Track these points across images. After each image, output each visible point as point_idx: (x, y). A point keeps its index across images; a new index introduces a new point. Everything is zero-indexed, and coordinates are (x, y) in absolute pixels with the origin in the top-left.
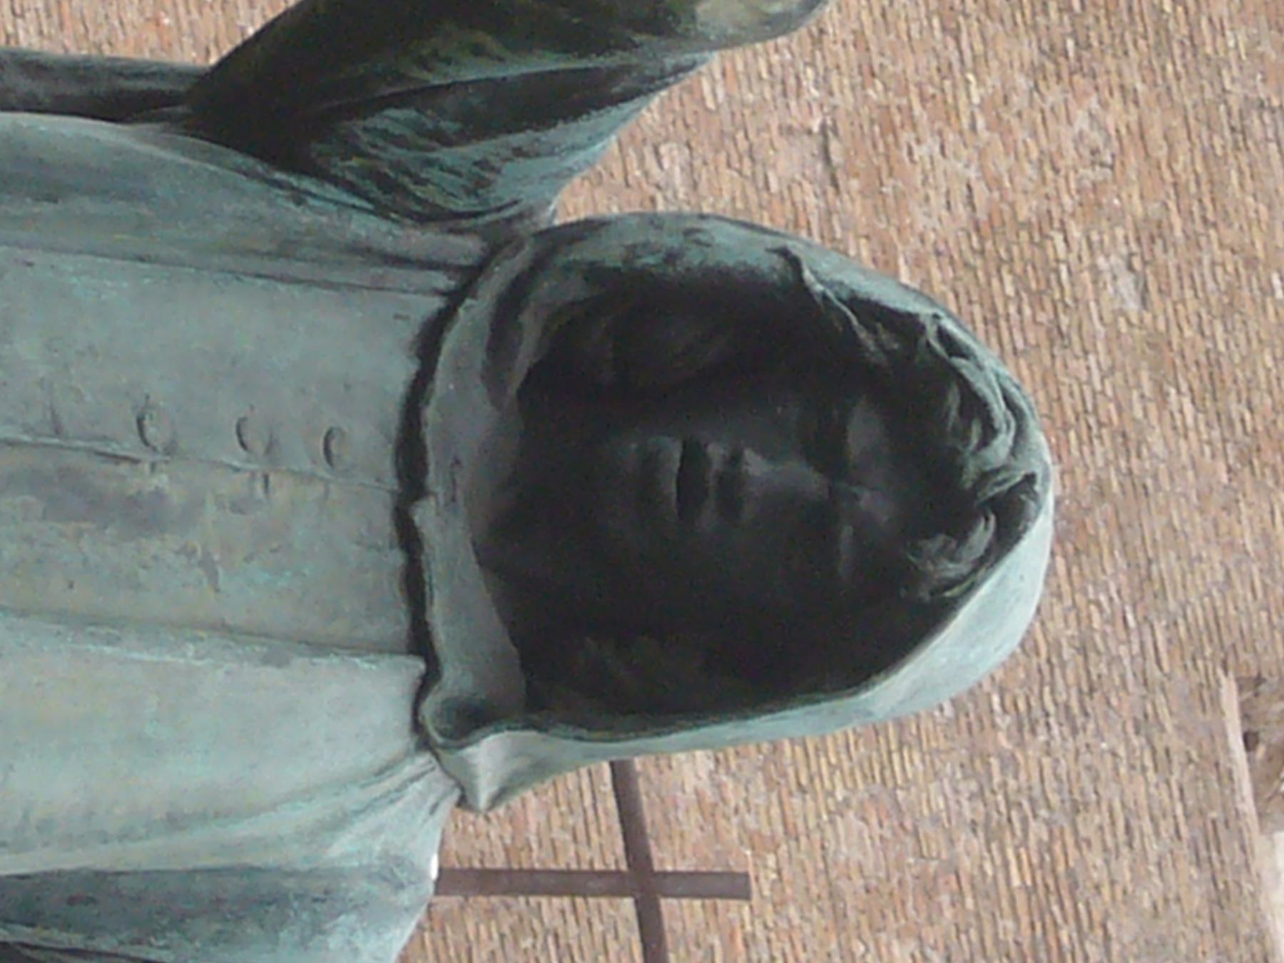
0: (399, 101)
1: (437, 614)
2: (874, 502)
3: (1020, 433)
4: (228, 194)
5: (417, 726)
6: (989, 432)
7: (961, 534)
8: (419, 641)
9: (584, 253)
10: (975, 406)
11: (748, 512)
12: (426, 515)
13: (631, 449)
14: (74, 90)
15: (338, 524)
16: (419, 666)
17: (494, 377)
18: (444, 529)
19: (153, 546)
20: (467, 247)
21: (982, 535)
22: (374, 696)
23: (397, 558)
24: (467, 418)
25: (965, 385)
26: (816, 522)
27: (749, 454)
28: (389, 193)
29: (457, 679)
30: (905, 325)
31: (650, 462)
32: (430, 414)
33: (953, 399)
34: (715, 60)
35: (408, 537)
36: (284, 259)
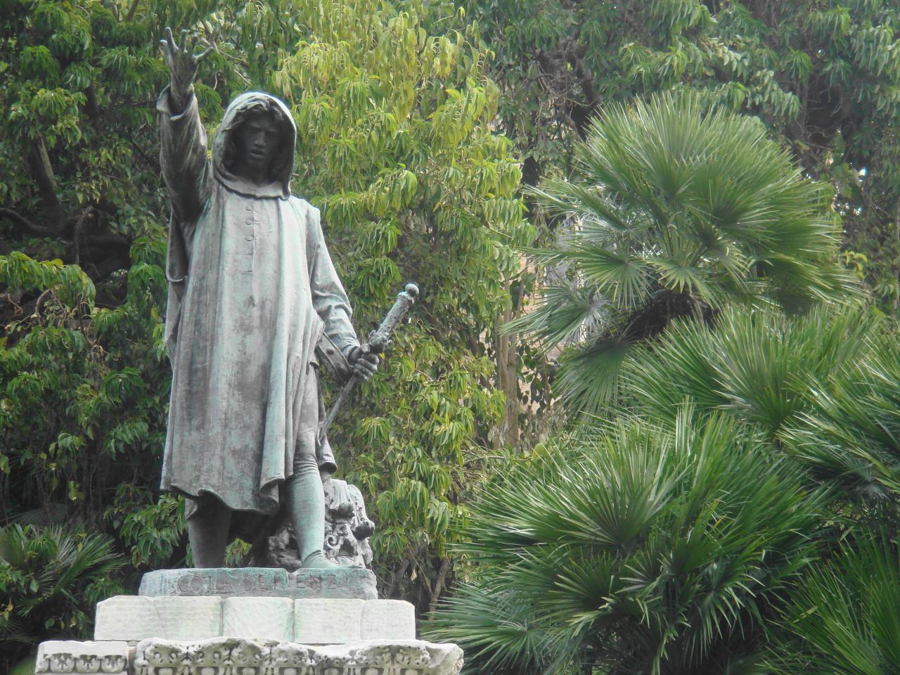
8: (276, 199)
9: (218, 164)
10: (256, 107)
20: (216, 182)
24: (240, 186)
27: (256, 142)
28: (209, 195)
29: (281, 193)
30: (238, 114)
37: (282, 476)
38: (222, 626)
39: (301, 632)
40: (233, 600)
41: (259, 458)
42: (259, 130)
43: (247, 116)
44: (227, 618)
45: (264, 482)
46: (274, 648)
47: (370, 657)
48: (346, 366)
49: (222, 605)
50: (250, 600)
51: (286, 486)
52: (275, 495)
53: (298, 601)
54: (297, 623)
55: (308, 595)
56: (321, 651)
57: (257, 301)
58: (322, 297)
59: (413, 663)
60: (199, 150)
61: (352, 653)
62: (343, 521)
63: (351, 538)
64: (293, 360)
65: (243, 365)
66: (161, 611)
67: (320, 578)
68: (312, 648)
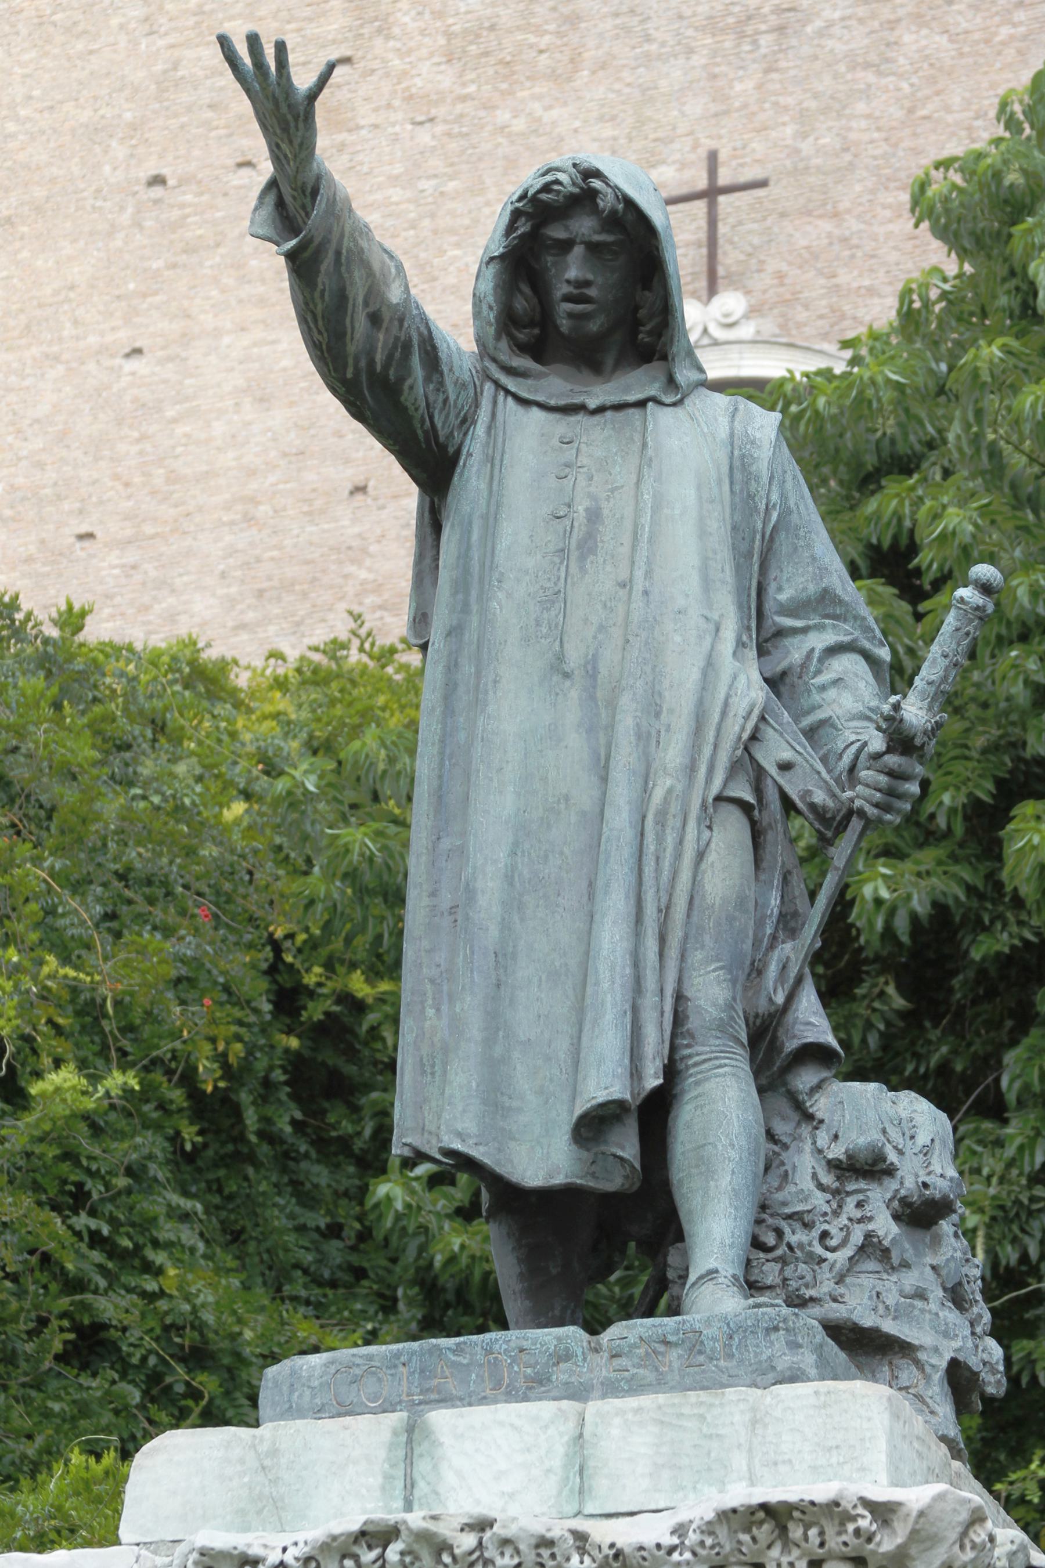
0: (431, 418)
1: (631, 398)
2: (584, 226)
3: (558, 169)
4: (471, 482)
5: (674, 405)
6: (557, 182)
7: (593, 193)
8: (641, 404)
9: (491, 343)
10: (546, 188)
11: (590, 277)
12: (592, 403)
13: (564, 325)
14: (430, 540)
15: (596, 438)
16: (650, 404)
17: (539, 376)
18: (597, 395)
19: (606, 512)
20: (488, 388)
21: (596, 184)
22: (666, 424)
23: (609, 414)
25: (539, 192)
26: (594, 248)
28: (467, 422)
30: (516, 214)
31: (571, 315)
32: (552, 402)
33: (544, 196)
34: (413, 291)
35: (601, 410)
36: (493, 460)
38: (410, 1485)
39: (601, 1484)
44: (422, 1466)
46: (488, 1535)
48: (833, 796)
49: (411, 1429)
50: (480, 1414)
51: (655, 1113)
52: (626, 1144)
53: (594, 1407)
54: (591, 1463)
55: (636, 1388)
58: (795, 631)
59: (834, 1542)
60: (386, 315)
61: (680, 1530)
62: (862, 1185)
63: (886, 1227)
64: (658, 795)
66: (267, 1462)
67: (666, 1343)
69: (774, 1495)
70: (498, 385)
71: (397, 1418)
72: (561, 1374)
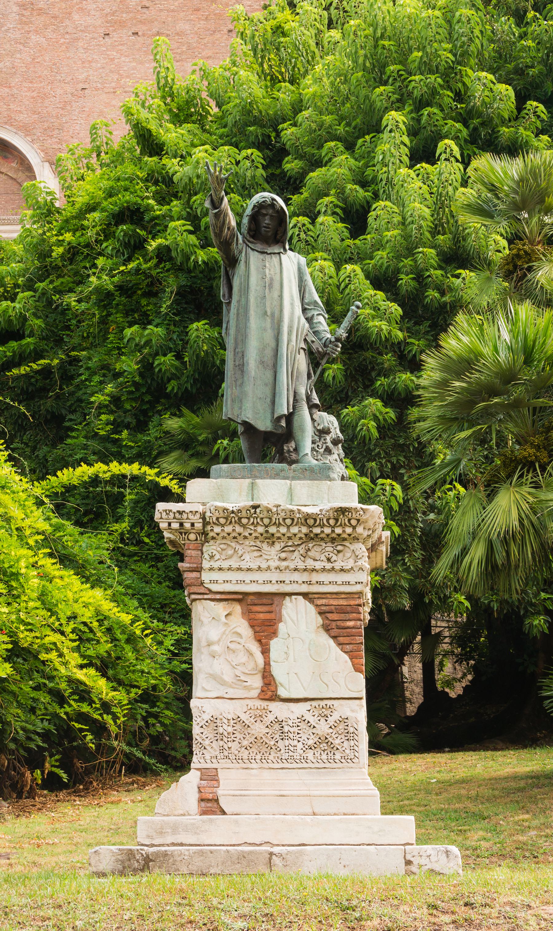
24: (259, 247)
28: (241, 252)
37: (286, 412)
38: (253, 495)
39: (295, 499)
40: (259, 481)
41: (273, 402)
42: (266, 215)
43: (260, 207)
44: (255, 492)
45: (276, 416)
47: (331, 512)
50: (268, 481)
53: (293, 482)
55: (299, 479)
56: (305, 510)
57: (269, 313)
59: (354, 516)
61: (321, 510)
65: (261, 351)
68: (299, 508)
69: (344, 505)
70: (247, 245)
71: (248, 481)
72: (282, 474)
